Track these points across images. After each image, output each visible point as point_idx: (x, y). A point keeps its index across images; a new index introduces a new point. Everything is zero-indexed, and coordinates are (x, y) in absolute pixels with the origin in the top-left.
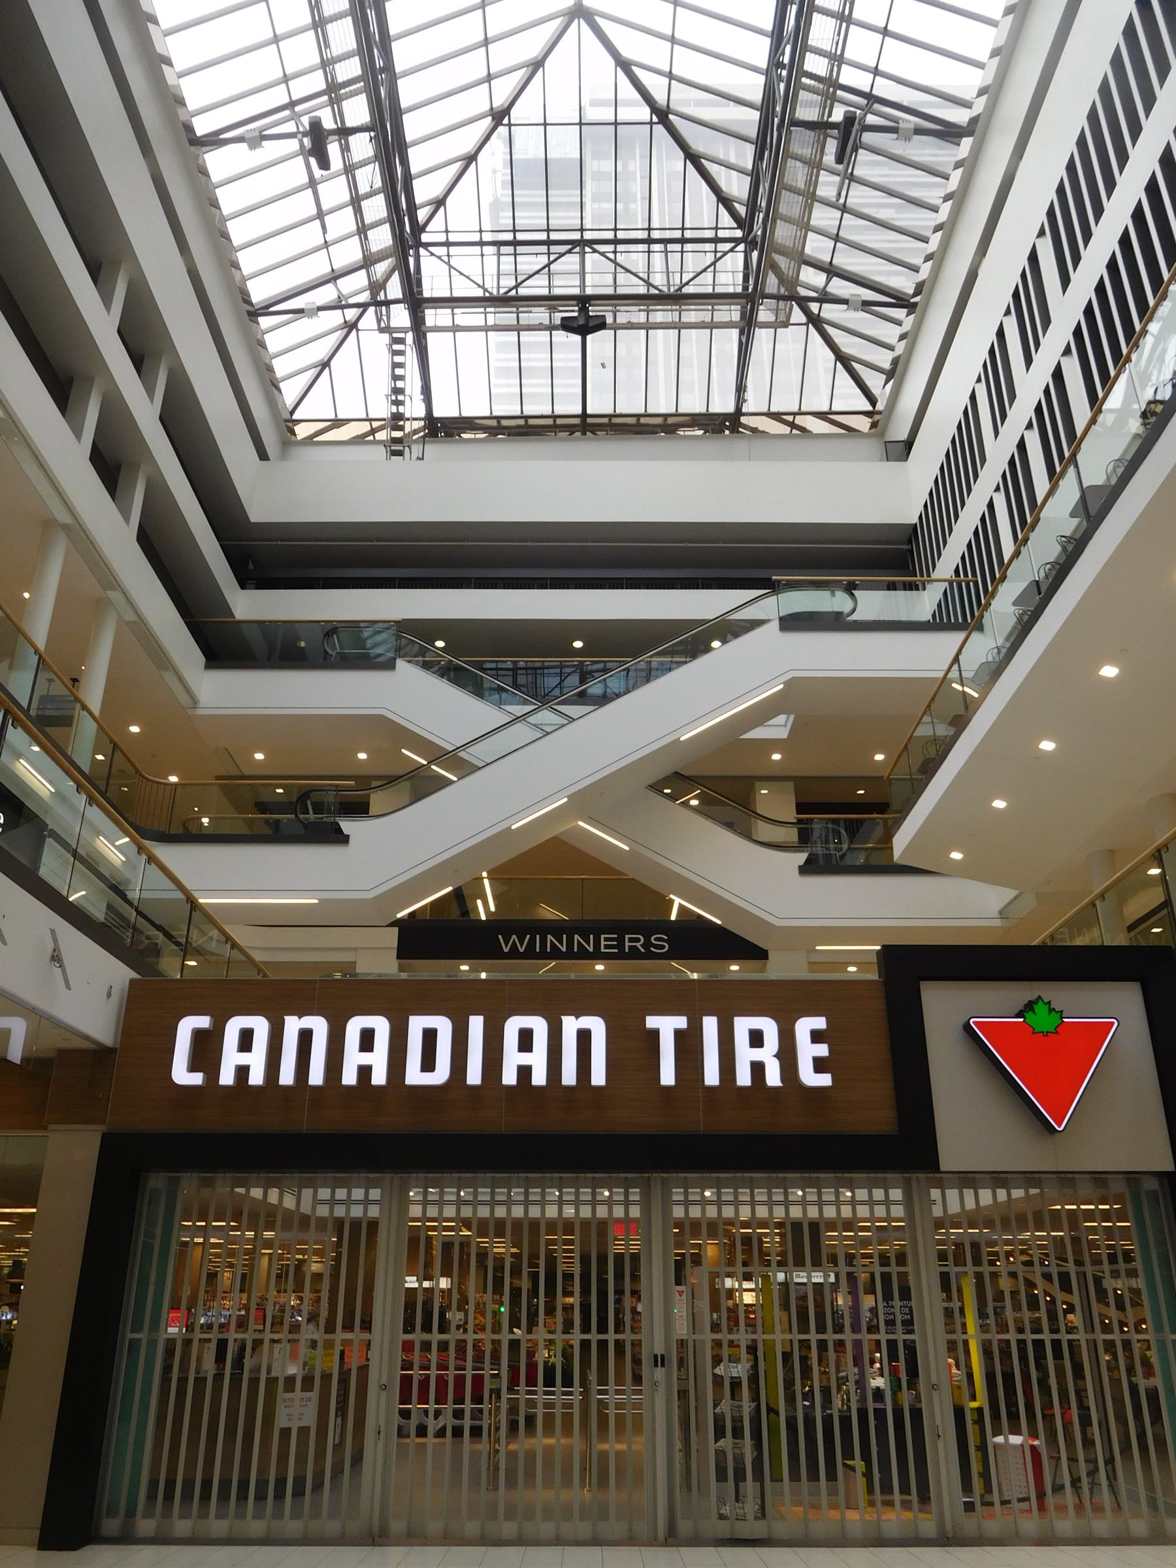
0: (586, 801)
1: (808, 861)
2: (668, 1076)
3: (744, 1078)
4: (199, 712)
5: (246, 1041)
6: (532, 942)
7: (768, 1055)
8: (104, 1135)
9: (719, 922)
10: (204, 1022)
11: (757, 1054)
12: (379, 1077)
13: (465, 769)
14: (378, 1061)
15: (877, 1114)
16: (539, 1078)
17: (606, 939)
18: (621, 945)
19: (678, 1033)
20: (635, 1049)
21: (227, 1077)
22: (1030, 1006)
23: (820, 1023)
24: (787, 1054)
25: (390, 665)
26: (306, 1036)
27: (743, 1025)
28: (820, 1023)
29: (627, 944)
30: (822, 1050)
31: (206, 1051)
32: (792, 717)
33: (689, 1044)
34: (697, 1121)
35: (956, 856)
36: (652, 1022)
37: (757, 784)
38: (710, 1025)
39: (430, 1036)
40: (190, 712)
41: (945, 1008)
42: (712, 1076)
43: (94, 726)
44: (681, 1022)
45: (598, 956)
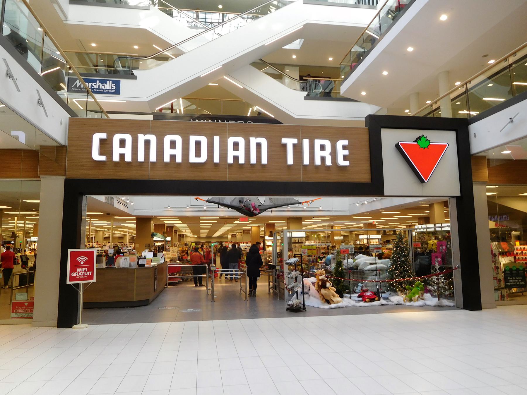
0: (230, 68)
1: (308, 95)
2: (290, 161)
3: (318, 162)
4: (68, 22)
5: (122, 143)
7: (327, 153)
8: (66, 181)
9: (273, 117)
10: (104, 136)
11: (323, 153)
12: (179, 159)
13: (179, 54)
14: (178, 153)
15: (363, 176)
16: (242, 161)
19: (294, 145)
20: (277, 150)
21: (116, 158)
22: (419, 138)
23: (346, 142)
26: (147, 143)
27: (318, 143)
28: (346, 142)
30: (346, 152)
31: (106, 146)
32: (303, 40)
33: (298, 149)
34: (301, 177)
35: (364, 93)
36: (284, 140)
37: (286, 67)
38: (306, 142)
39: (198, 144)
40: (65, 22)
41: (390, 138)
42: (306, 161)
43: (26, 20)
44: (295, 141)
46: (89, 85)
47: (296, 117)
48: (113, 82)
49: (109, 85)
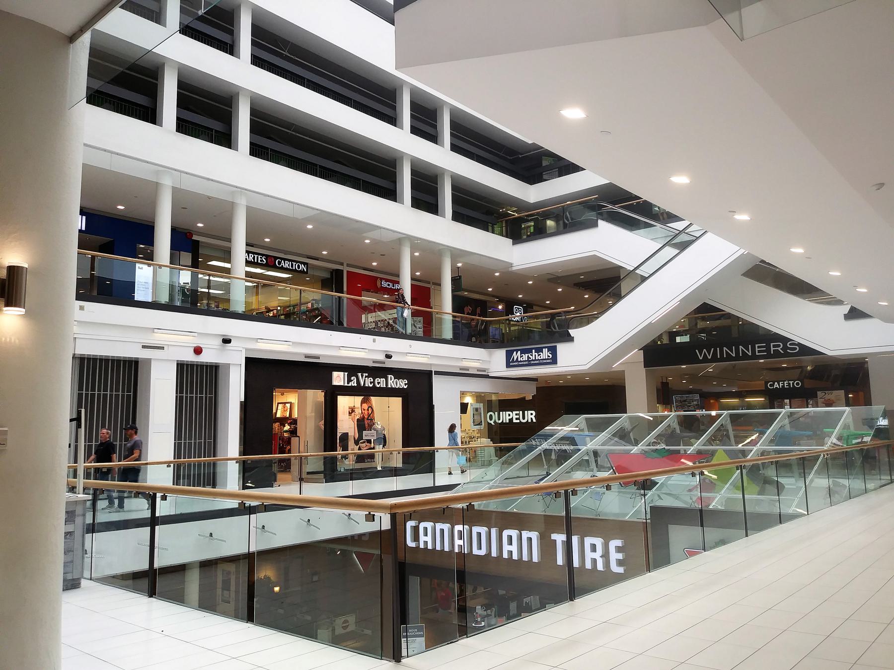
2: (560, 560)
3: (588, 566)
4: (514, 268)
6: (715, 351)
7: (598, 555)
17: (759, 347)
18: (768, 349)
20: (548, 547)
23: (618, 543)
24: (606, 556)
25: (594, 225)
28: (618, 543)
29: (772, 349)
30: (620, 556)
36: (554, 536)
45: (754, 357)
46: (525, 357)
47: (830, 353)
48: (549, 349)
49: (545, 354)
